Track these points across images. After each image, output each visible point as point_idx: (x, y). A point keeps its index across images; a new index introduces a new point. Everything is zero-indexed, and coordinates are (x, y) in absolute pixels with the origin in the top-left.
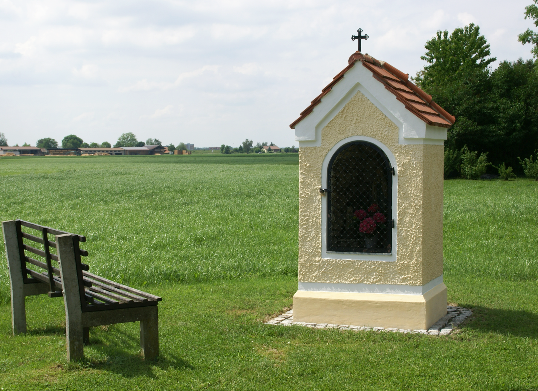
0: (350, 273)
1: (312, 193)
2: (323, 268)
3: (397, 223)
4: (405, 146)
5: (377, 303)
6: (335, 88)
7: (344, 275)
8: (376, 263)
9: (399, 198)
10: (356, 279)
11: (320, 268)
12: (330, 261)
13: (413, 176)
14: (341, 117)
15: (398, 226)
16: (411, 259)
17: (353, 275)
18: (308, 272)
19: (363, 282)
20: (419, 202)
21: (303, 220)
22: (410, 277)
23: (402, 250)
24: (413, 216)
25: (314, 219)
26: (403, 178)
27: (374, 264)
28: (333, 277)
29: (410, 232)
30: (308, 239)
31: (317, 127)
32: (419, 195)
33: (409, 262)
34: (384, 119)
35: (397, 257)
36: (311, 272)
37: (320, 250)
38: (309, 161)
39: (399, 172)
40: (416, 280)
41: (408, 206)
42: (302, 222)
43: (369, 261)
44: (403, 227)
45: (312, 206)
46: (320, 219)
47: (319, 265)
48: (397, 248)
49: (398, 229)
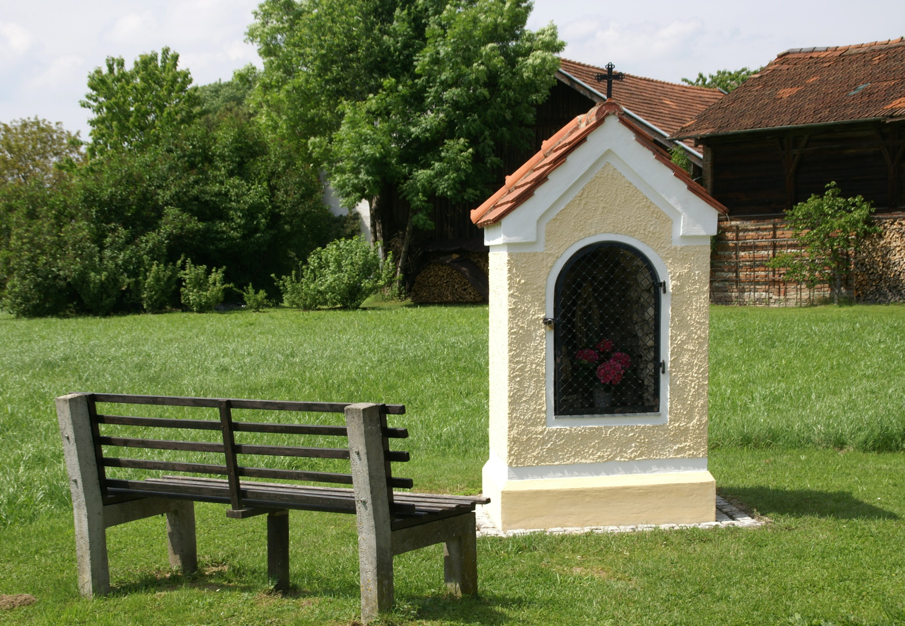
0: (594, 447)
1: (529, 326)
2: (549, 443)
3: (669, 365)
4: (682, 249)
5: (640, 488)
6: (571, 158)
7: (583, 451)
8: (636, 428)
9: (673, 328)
10: (603, 456)
11: (544, 442)
12: (560, 431)
13: (694, 294)
14: (579, 204)
15: (671, 371)
16: (691, 418)
17: (598, 450)
18: (523, 450)
19: (614, 459)
20: (704, 332)
21: (514, 369)
22: (689, 446)
23: (676, 406)
24: (694, 354)
25: (534, 366)
26: (678, 297)
27: (632, 430)
28: (565, 455)
29: (689, 378)
30: (524, 399)
31: (539, 221)
32: (704, 322)
33: (688, 423)
34: (649, 207)
35: (668, 416)
36: (529, 450)
37: (543, 415)
38: (524, 275)
39: (672, 289)
40: (697, 450)
41: (686, 339)
42: (513, 372)
43: (624, 427)
44: (679, 371)
45: (529, 347)
46: (543, 366)
47: (543, 438)
48: (669, 403)
49: (671, 374)
